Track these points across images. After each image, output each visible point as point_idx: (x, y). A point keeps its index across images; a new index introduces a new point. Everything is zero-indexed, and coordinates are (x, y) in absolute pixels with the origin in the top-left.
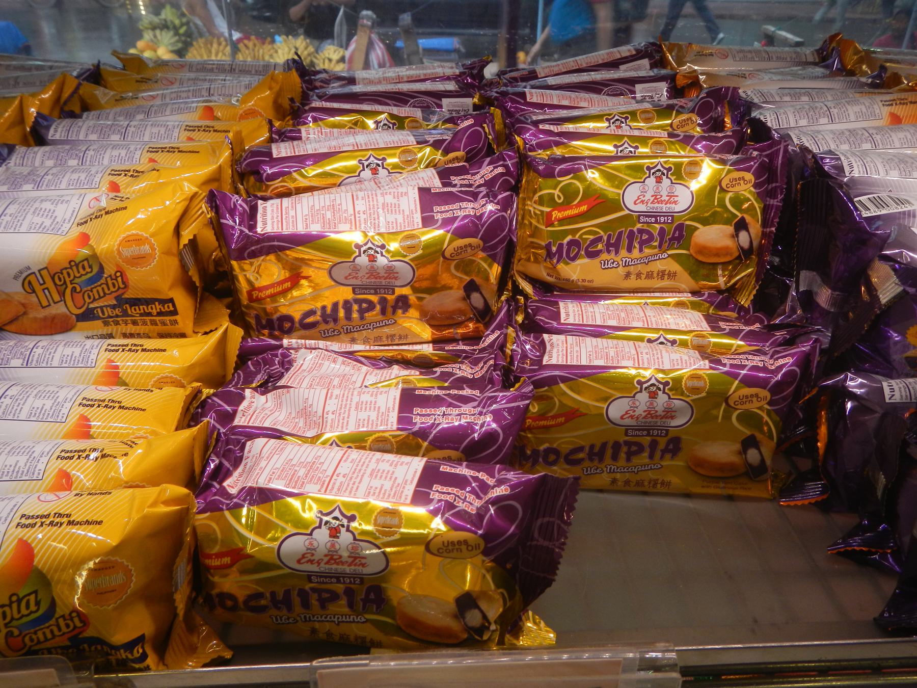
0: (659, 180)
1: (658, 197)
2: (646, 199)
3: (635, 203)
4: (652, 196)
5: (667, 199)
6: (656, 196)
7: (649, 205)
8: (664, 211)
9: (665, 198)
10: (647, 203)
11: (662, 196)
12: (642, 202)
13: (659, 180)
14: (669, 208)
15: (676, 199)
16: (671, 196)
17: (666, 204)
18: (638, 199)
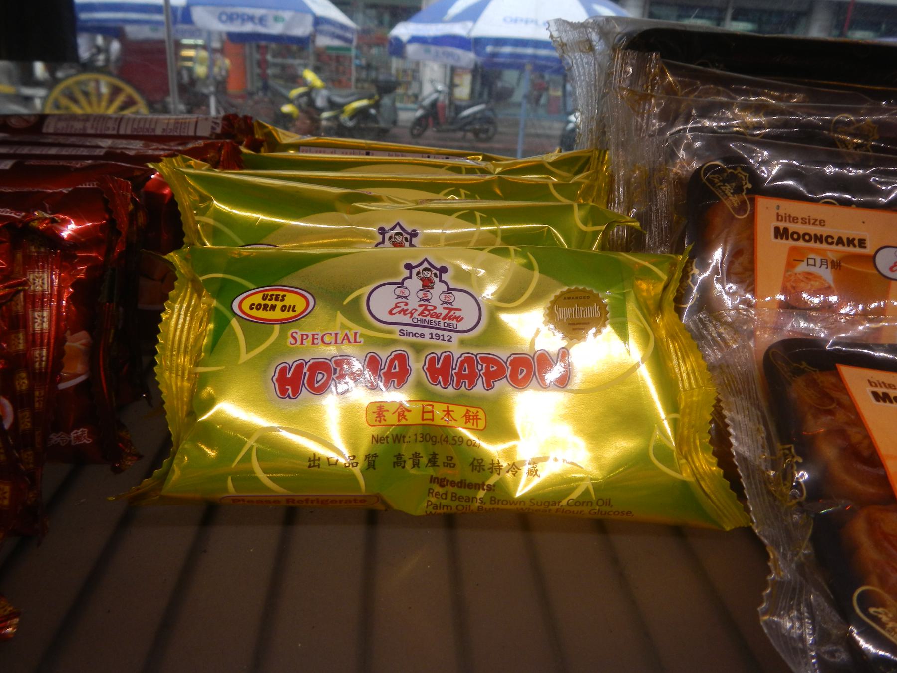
0: (427, 284)
1: (429, 308)
2: (410, 307)
3: (391, 313)
4: (420, 306)
5: (445, 312)
6: (426, 306)
7: (415, 315)
8: (442, 326)
9: (440, 309)
10: (412, 314)
11: (435, 308)
12: (404, 311)
13: (427, 284)
14: (449, 324)
15: (458, 313)
16: (451, 309)
17: (444, 318)
18: (396, 306)
